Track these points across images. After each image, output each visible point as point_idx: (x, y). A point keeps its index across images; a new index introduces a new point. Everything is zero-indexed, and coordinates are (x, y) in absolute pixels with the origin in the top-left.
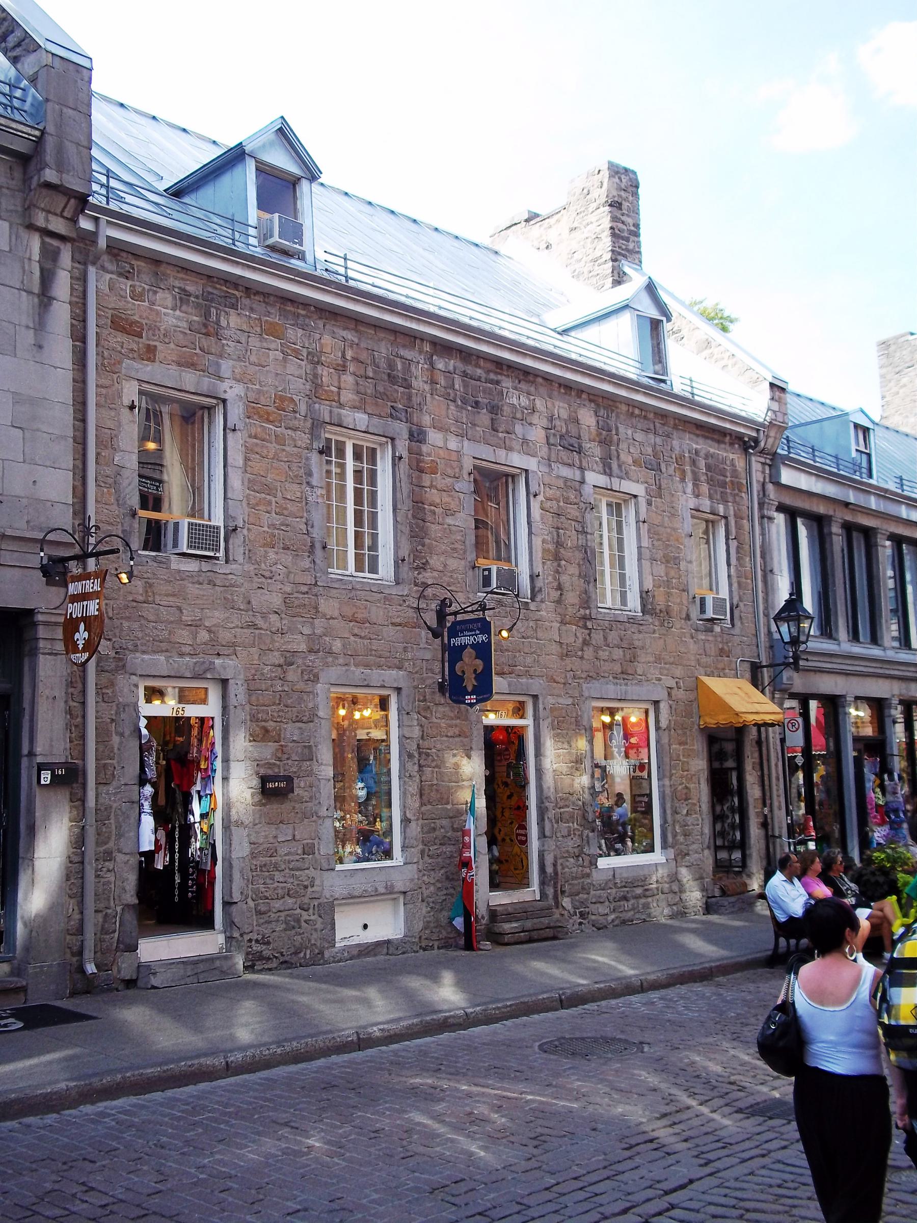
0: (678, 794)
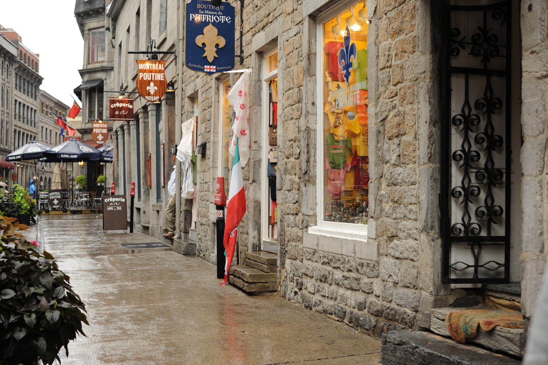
0: (388, 125)
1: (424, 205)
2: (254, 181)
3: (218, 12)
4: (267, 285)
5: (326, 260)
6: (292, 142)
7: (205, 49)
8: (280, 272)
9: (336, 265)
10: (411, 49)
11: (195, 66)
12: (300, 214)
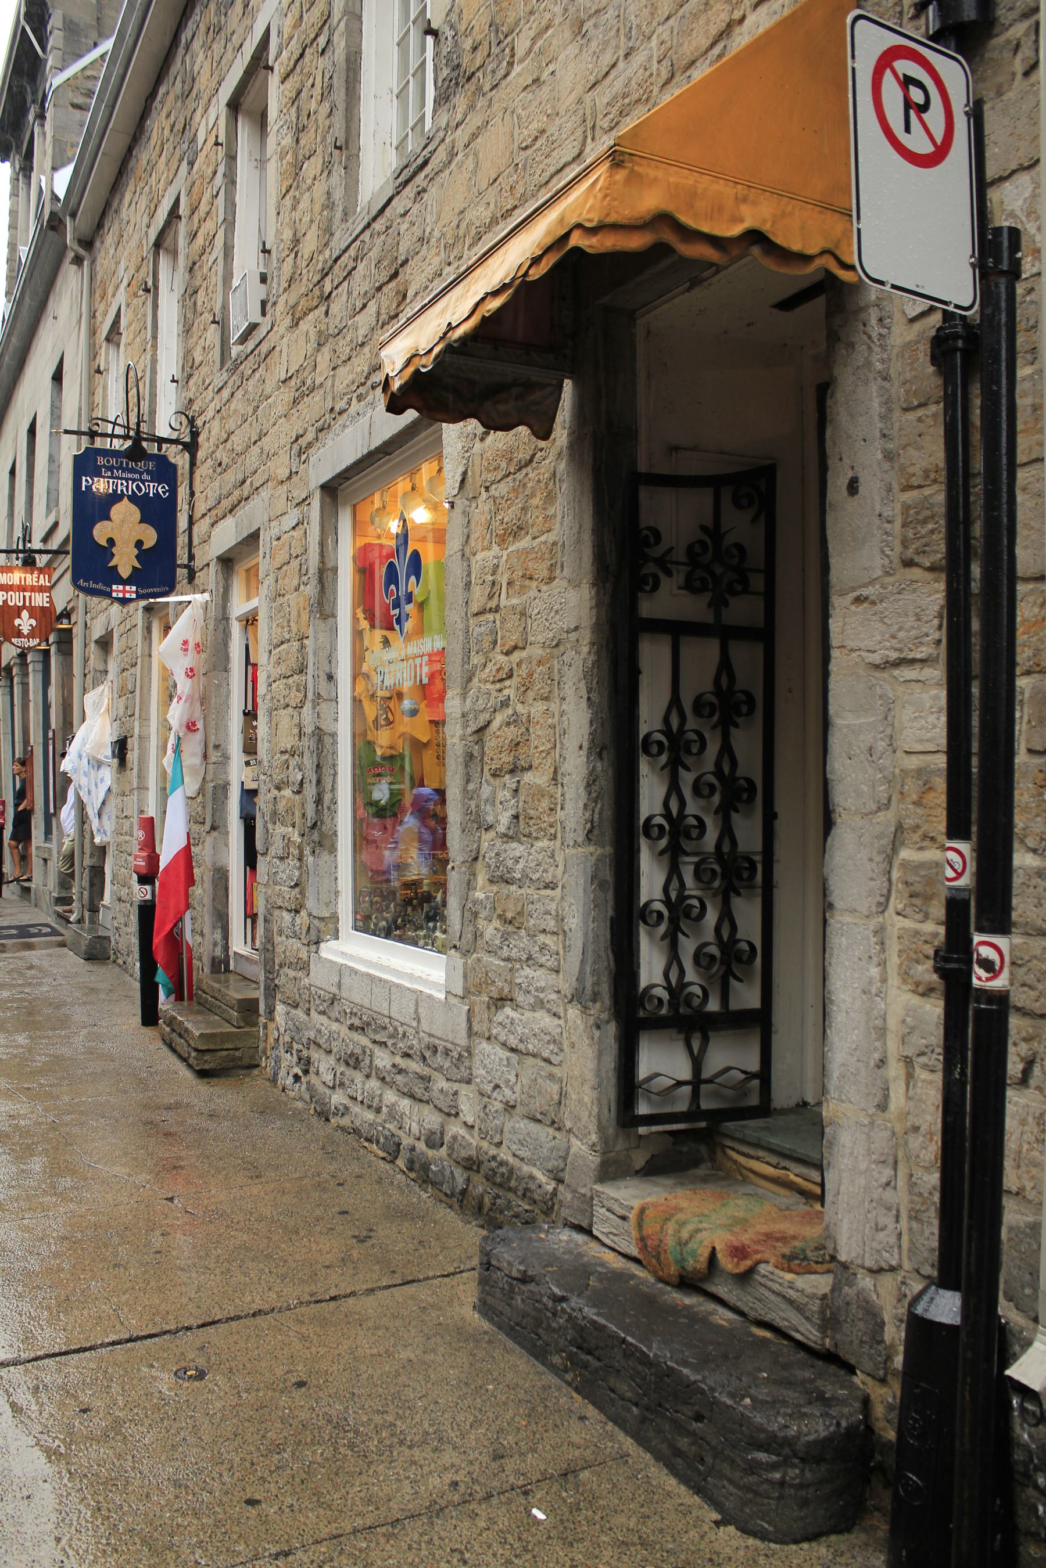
0: (491, 744)
1: (577, 941)
2: (213, 828)
3: (141, 474)
4: (237, 1054)
5: (357, 1022)
6: (287, 756)
7: (114, 550)
8: (265, 1027)
9: (378, 1038)
10: (546, 573)
11: (92, 585)
12: (303, 913)
